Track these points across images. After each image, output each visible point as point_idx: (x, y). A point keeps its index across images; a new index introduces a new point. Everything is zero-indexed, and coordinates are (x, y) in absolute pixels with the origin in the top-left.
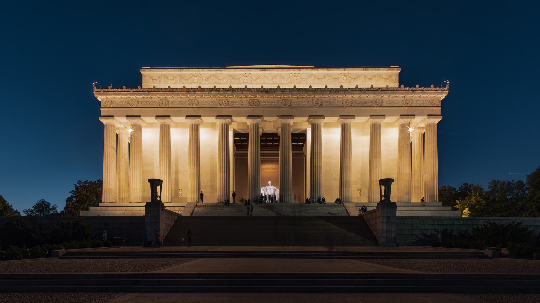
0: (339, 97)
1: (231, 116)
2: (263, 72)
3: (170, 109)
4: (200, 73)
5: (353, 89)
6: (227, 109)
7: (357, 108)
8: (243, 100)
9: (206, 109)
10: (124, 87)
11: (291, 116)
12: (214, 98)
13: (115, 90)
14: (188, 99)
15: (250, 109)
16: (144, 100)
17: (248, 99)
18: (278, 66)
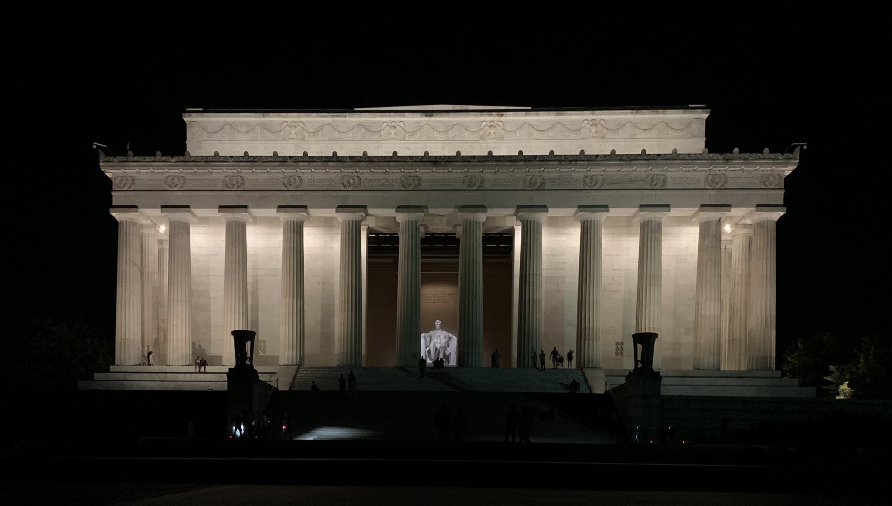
0: (578, 173)
1: (365, 207)
2: (428, 119)
3: (247, 194)
4: (303, 119)
5: (605, 156)
6: (357, 193)
7: (613, 192)
8: (387, 176)
9: (317, 193)
10: (158, 152)
11: (482, 208)
12: (333, 174)
13: (141, 158)
14: (282, 175)
15: (402, 193)
16: (197, 177)
17: (399, 176)
18: (458, 107)
